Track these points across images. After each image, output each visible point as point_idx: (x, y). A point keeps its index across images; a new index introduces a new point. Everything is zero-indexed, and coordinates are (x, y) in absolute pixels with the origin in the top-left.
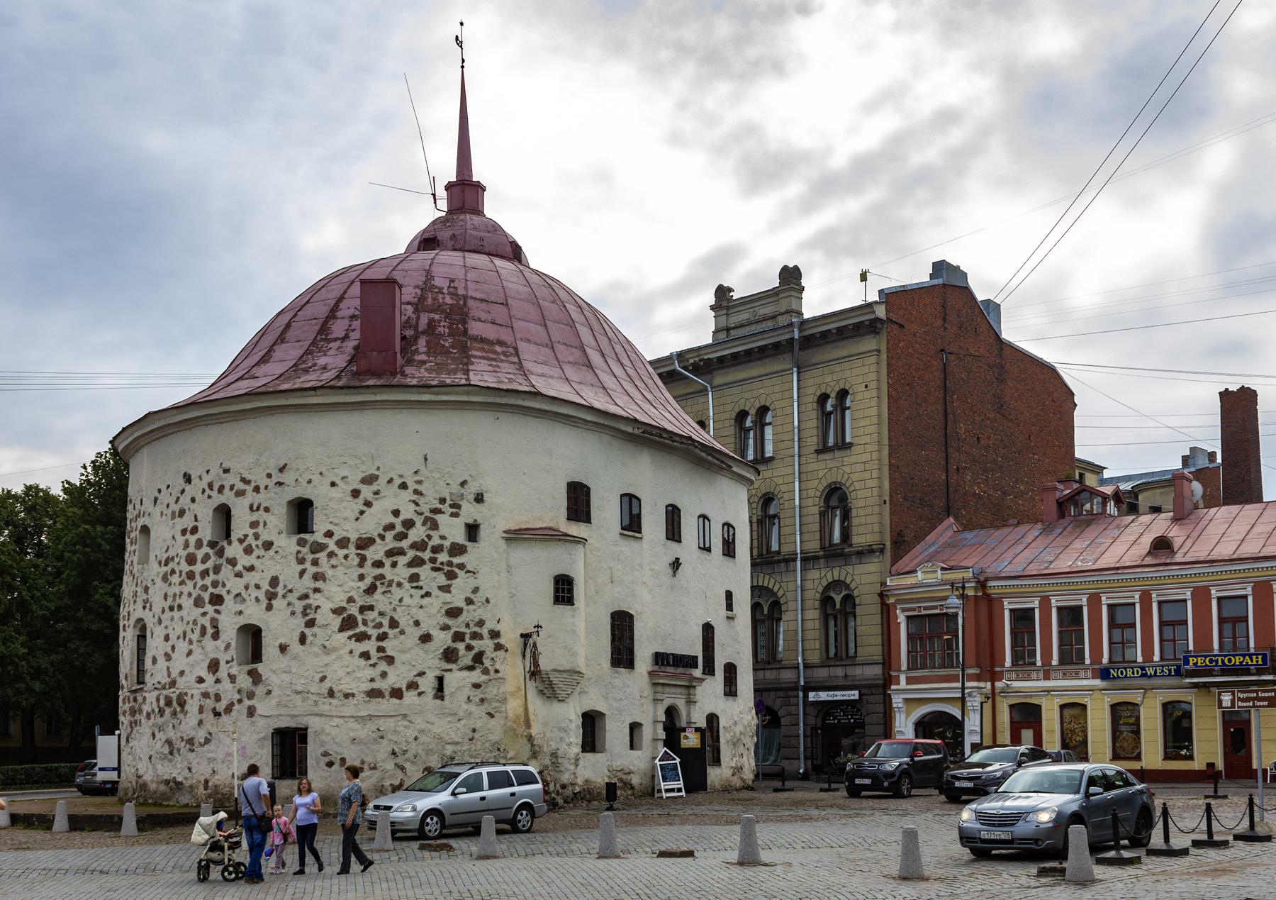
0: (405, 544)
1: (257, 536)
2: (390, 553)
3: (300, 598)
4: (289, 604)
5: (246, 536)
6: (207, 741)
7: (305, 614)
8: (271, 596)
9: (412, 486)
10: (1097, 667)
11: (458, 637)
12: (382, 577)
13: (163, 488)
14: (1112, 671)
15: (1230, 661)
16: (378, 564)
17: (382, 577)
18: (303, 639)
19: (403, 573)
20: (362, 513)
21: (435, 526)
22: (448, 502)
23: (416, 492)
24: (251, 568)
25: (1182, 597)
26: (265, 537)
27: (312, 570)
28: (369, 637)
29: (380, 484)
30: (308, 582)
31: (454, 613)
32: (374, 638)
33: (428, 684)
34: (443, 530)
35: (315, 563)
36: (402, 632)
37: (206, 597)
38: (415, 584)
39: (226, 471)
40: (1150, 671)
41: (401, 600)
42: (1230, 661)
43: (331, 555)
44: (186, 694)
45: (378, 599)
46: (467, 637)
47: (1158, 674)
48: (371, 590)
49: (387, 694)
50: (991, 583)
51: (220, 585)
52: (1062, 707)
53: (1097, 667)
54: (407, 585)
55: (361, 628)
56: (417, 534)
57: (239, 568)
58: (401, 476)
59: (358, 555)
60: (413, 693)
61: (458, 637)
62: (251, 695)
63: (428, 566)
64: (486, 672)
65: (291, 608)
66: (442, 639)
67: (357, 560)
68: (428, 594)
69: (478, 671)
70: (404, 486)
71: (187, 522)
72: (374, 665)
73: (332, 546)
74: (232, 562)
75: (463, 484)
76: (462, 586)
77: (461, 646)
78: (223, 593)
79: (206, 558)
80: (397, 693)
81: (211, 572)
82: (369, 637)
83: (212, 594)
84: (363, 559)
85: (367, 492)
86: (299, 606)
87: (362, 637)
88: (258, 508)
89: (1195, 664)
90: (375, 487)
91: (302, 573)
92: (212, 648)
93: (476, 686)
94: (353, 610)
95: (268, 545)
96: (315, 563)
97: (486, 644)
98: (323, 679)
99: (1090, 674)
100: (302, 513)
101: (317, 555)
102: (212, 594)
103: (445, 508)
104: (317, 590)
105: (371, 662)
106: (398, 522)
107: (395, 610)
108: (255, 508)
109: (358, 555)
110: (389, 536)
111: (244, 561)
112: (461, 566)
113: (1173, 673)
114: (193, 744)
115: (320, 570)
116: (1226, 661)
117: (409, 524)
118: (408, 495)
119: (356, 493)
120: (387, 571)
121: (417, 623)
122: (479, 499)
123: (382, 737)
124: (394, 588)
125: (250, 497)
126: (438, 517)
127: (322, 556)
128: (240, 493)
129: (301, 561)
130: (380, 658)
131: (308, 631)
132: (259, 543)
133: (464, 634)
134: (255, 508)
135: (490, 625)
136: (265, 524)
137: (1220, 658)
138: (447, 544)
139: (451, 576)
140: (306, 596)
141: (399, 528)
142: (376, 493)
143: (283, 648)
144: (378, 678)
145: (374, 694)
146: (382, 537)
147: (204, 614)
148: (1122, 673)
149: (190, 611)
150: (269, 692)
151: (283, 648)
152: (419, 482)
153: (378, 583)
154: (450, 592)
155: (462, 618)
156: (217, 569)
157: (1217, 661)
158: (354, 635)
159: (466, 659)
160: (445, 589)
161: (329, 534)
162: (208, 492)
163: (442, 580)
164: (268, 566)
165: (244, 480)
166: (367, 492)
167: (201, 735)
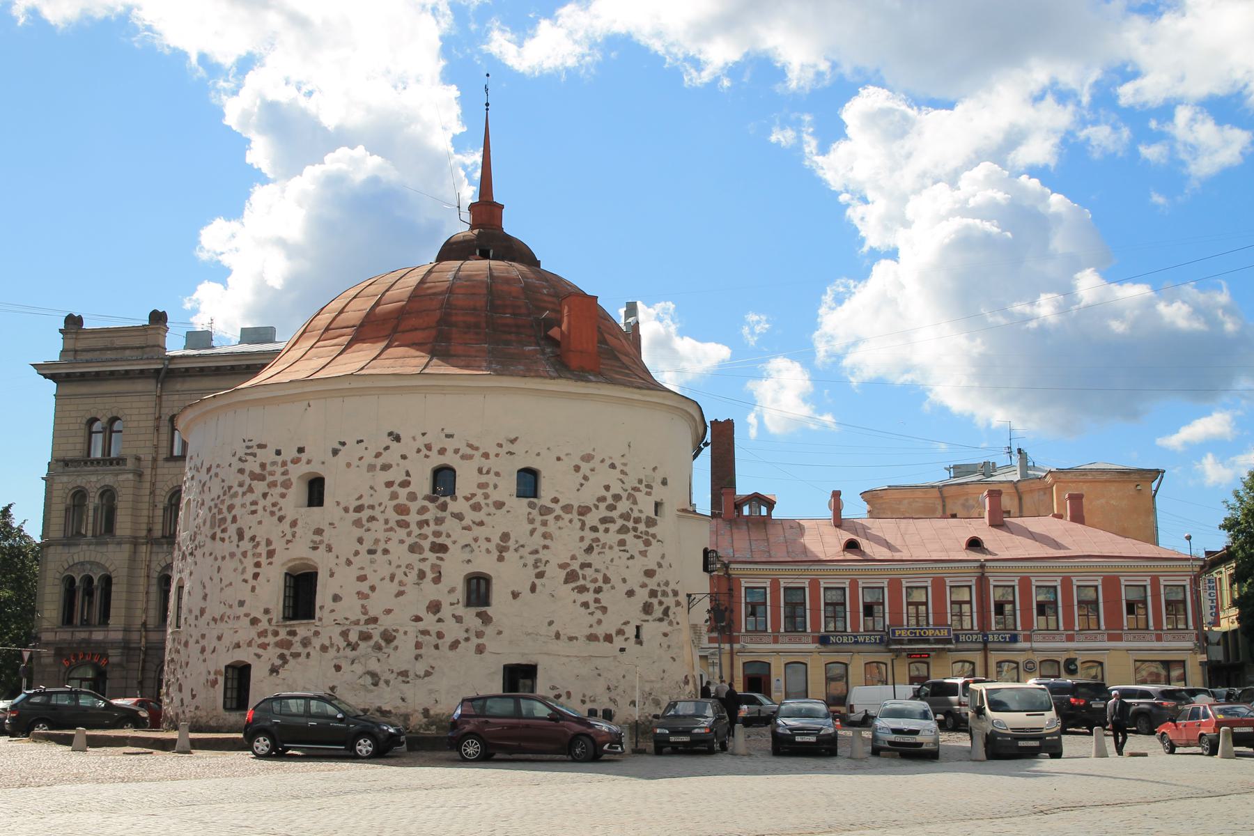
0: (615, 514)
1: (486, 496)
2: (604, 520)
3: (532, 553)
4: (521, 557)
5: (473, 495)
6: (428, 674)
7: (536, 566)
8: (502, 550)
9: (619, 467)
10: (817, 634)
11: (653, 594)
12: (597, 540)
13: (351, 442)
14: (831, 638)
15: (925, 633)
16: (594, 529)
17: (597, 540)
18: (533, 589)
19: (612, 538)
20: (582, 485)
21: (635, 502)
22: (644, 483)
23: (623, 472)
24: (481, 524)
25: (882, 585)
26: (496, 496)
27: (541, 530)
28: (588, 590)
29: (595, 463)
30: (538, 540)
31: (649, 573)
32: (591, 590)
33: (630, 631)
34: (640, 506)
35: (544, 523)
36: (613, 588)
37: (426, 545)
38: (622, 548)
39: (449, 436)
40: (861, 639)
41: (612, 560)
42: (925, 633)
43: (558, 518)
44: (396, 631)
45: (593, 558)
46: (659, 594)
47: (867, 641)
48: (589, 550)
49: (601, 638)
50: (732, 566)
51: (444, 535)
52: (786, 664)
53: (817, 634)
54: (616, 548)
55: (581, 582)
56: (623, 506)
57: (467, 522)
58: (611, 458)
59: (580, 520)
60: (621, 638)
61: (653, 594)
62: (479, 635)
63: (632, 533)
64: (671, 623)
65: (522, 561)
66: (642, 595)
67: (579, 524)
68: (632, 557)
69: (665, 623)
70: (613, 466)
71: (396, 475)
72: (592, 614)
73: (558, 512)
74: (459, 517)
75: (654, 469)
76: (654, 550)
77: (655, 601)
78: (448, 542)
79: (423, 510)
80: (608, 638)
81: (432, 523)
82: (588, 590)
83: (433, 544)
84: (583, 524)
85: (585, 468)
86: (530, 560)
87: (582, 589)
88: (488, 472)
89: (900, 635)
90: (591, 465)
91: (532, 532)
92: (431, 591)
93: (665, 635)
94: (575, 566)
95: (499, 505)
96: (544, 523)
97: (669, 601)
98: (551, 623)
99: (810, 639)
100: (529, 481)
101: (545, 518)
102: (433, 544)
103: (642, 487)
104: (546, 547)
105: (589, 611)
106: (609, 495)
107: (607, 568)
108: (484, 471)
109: (580, 520)
110: (602, 506)
111: (470, 516)
112: (654, 536)
113: (878, 641)
114: (407, 676)
115: (548, 530)
116: (923, 634)
117: (617, 497)
118: (616, 473)
119: (577, 468)
120: (600, 535)
121: (624, 581)
122: (664, 482)
123: (599, 675)
124: (607, 550)
125: (478, 461)
126: (636, 494)
127: (550, 518)
128: (470, 457)
129: (531, 521)
130: (597, 608)
131: (538, 582)
132: (490, 501)
133: (657, 591)
134: (484, 471)
135: (672, 586)
136: (495, 486)
137: (918, 631)
138: (643, 517)
139: (647, 543)
140: (536, 552)
141: (610, 501)
142: (592, 470)
143: (515, 595)
144: (595, 625)
145: (592, 638)
146: (597, 507)
147: (424, 560)
148: (839, 640)
149: (400, 553)
150: (500, 633)
151: (515, 595)
152: (625, 465)
153: (594, 545)
154: (646, 556)
155: (656, 579)
156: (439, 521)
157: (915, 633)
158: (577, 588)
159: (658, 611)
160: (644, 553)
161: (555, 500)
162: (424, 451)
163: (642, 548)
164: (498, 524)
165: (470, 446)
166: (585, 468)
167: (421, 668)
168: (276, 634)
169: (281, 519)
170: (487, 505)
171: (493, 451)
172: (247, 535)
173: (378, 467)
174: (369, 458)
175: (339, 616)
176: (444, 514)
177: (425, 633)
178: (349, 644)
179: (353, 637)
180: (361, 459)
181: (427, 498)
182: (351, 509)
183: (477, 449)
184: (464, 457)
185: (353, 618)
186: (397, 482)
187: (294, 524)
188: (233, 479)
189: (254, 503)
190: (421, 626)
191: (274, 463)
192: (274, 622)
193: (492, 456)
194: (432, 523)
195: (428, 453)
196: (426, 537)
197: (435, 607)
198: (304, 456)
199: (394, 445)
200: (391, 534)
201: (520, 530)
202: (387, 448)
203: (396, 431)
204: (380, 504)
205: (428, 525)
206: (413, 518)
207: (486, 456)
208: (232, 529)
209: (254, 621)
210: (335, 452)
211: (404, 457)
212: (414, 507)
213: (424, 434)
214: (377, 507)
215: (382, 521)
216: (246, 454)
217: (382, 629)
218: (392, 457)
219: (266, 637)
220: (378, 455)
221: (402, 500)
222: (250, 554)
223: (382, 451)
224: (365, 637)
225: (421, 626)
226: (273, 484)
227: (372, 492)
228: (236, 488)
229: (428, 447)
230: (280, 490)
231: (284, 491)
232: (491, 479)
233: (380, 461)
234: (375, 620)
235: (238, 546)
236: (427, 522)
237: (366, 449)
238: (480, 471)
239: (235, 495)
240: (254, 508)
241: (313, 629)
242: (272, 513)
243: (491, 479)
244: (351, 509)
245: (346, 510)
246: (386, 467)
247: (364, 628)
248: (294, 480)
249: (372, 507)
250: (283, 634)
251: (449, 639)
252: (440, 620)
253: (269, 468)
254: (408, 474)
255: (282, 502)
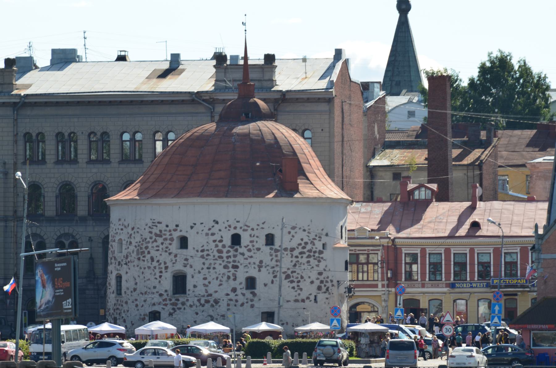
1: (253, 246)
5: (248, 246)
24: (251, 257)
26: (257, 246)
30: (274, 263)
44: (219, 299)
57: (246, 256)
62: (252, 300)
74: (243, 254)
79: (228, 252)
81: (232, 257)
88: (254, 236)
95: (258, 249)
108: (252, 236)
111: (247, 254)
125: (250, 232)
128: (246, 230)
136: (257, 242)
140: (273, 267)
156: (235, 256)
162: (228, 228)
165: (247, 226)
168: (170, 300)
169: (170, 254)
170: (254, 249)
171: (255, 228)
172: (156, 260)
173: (210, 234)
174: (206, 231)
175: (197, 293)
176: (236, 253)
177: (231, 300)
178: (201, 304)
179: (203, 302)
180: (203, 230)
181: (229, 247)
182: (199, 251)
183: (249, 227)
184: (244, 230)
185: (202, 294)
186: (218, 240)
187: (176, 256)
188: (147, 235)
189: (158, 246)
190: (229, 297)
191: (165, 231)
192: (169, 295)
193: (255, 229)
194: (232, 257)
195: (230, 229)
196: (230, 262)
197: (234, 290)
198: (179, 229)
199: (216, 225)
200: (216, 261)
201: (267, 260)
202: (213, 226)
203: (217, 220)
204: (211, 249)
205: (231, 258)
206: (224, 255)
207: (253, 229)
208: (148, 257)
209: (161, 295)
210: (192, 227)
211: (220, 230)
212: (225, 250)
213: (228, 221)
214: (210, 250)
215: (212, 256)
216: (153, 225)
217: (214, 299)
218: (215, 230)
219: (166, 301)
220: (210, 229)
221: (220, 247)
222: (157, 267)
223: (211, 228)
224: (207, 302)
225: (229, 297)
226: (166, 239)
227: (208, 244)
228: (148, 240)
229: (230, 226)
230: (168, 242)
231: (170, 242)
232: (255, 239)
233: (210, 232)
234: (211, 295)
235: (151, 264)
236: (230, 257)
237: (205, 226)
238: (251, 236)
239: (149, 242)
240: (157, 248)
241: (186, 299)
242: (166, 251)
243: (255, 239)
244: (199, 251)
245: (197, 251)
246: (213, 234)
247: (207, 298)
248: (175, 238)
249: (208, 250)
250: (173, 300)
251: (240, 303)
252: (236, 295)
253: (163, 232)
254: (222, 237)
255: (170, 247)
